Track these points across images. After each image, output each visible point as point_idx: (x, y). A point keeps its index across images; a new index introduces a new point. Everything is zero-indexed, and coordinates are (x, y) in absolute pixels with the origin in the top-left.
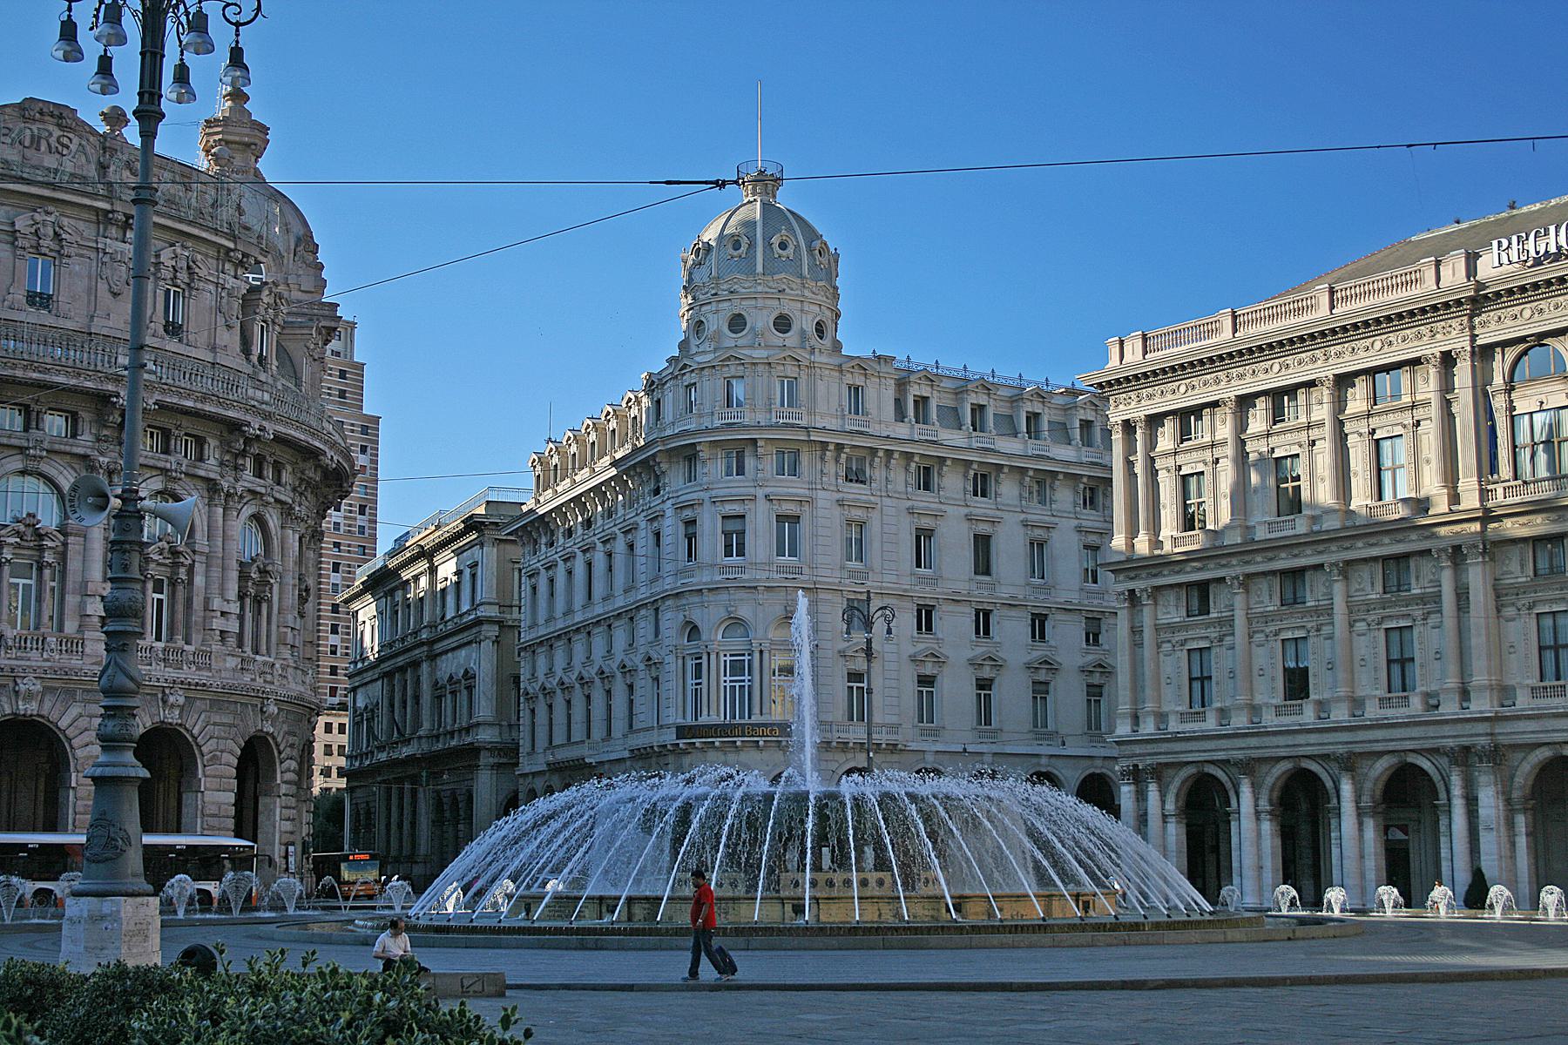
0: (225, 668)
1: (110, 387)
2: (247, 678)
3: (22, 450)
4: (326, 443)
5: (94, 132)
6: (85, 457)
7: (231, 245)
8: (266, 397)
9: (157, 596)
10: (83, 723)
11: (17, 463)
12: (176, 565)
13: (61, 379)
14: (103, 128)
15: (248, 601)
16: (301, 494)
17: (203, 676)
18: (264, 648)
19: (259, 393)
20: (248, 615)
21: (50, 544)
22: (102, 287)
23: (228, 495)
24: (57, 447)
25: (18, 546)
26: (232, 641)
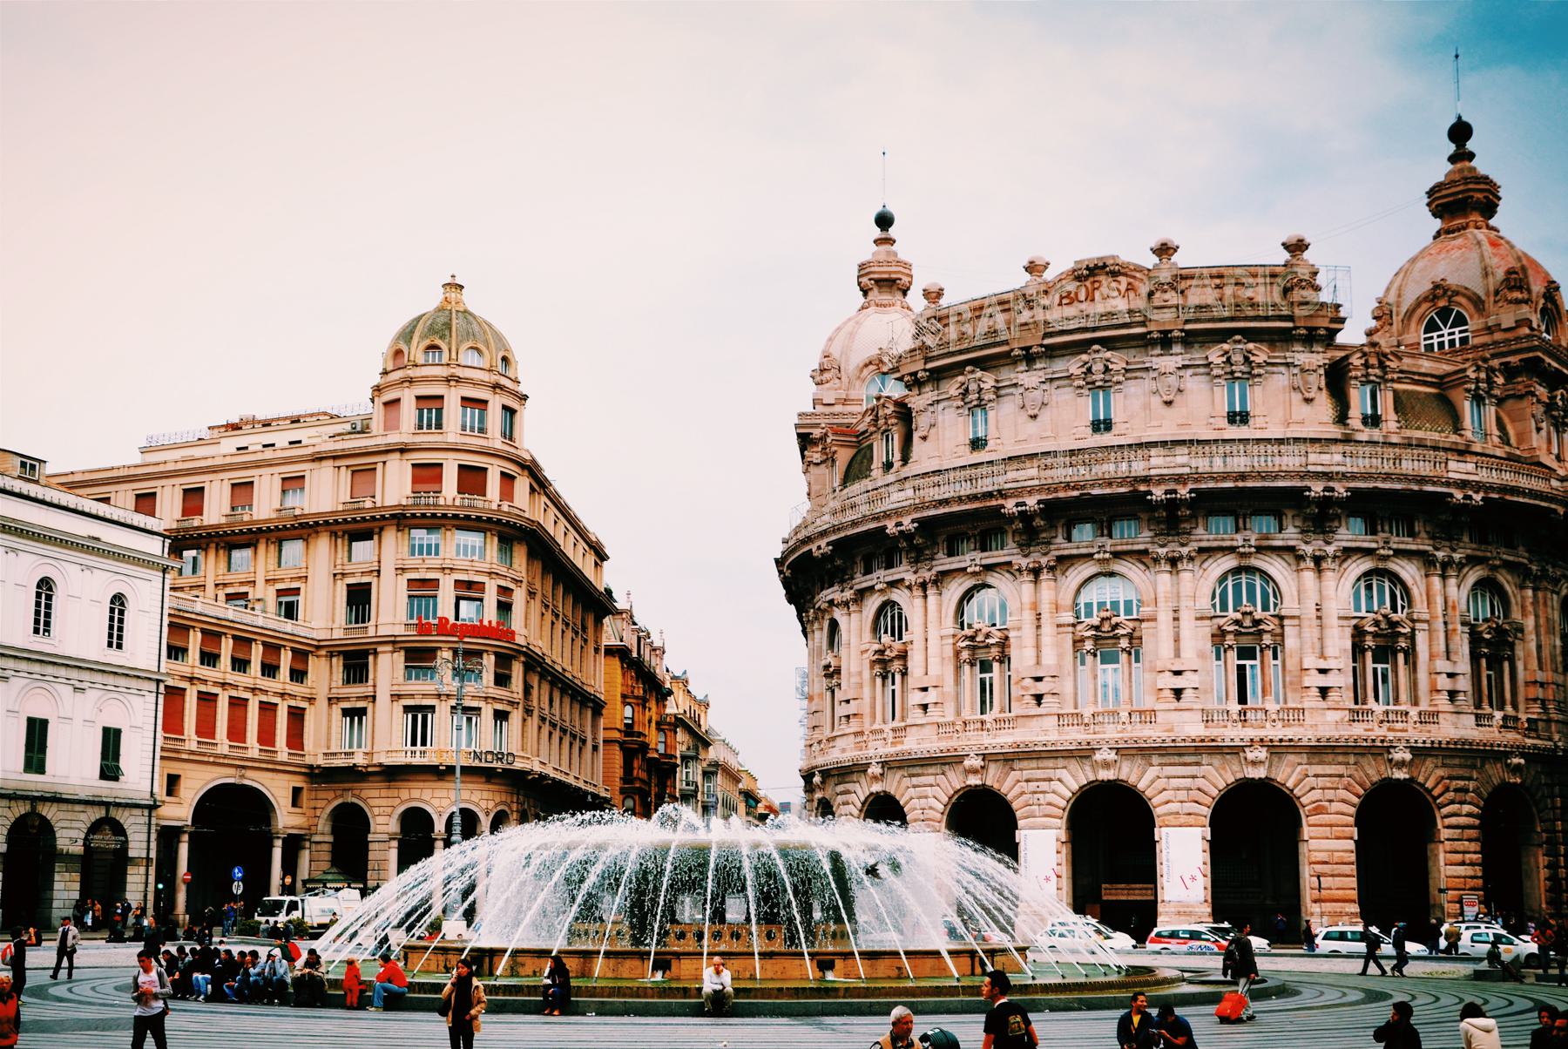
0: (1328, 723)
1: (1142, 488)
3: (1090, 556)
4: (1448, 484)
5: (1139, 269)
6: (1146, 552)
7: (1290, 325)
8: (1338, 458)
9: (1248, 663)
10: (1161, 783)
11: (1089, 569)
12: (1260, 633)
13: (1096, 491)
14: (1150, 261)
15: (1369, 655)
16: (1450, 540)
18: (1403, 696)
19: (1325, 458)
20: (1370, 665)
21: (1120, 631)
22: (1156, 401)
24: (1119, 548)
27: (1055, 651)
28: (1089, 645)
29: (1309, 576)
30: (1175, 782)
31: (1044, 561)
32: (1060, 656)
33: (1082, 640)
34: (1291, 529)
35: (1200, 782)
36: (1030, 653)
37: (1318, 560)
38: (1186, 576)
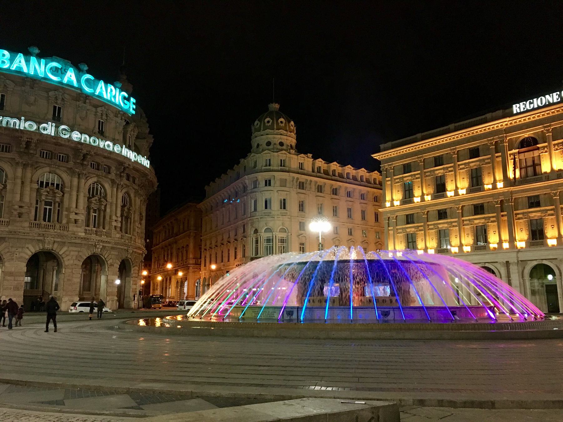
2: (123, 240)
9: (94, 214)
10: (67, 253)
11: (47, 169)
15: (124, 218)
17: (108, 239)
20: (124, 222)
23: (118, 185)
25: (47, 195)
26: (118, 229)
27: (29, 196)
28: (43, 198)
29: (115, 189)
30: (72, 253)
31: (30, 162)
32: (30, 199)
33: (41, 195)
34: (113, 174)
35: (81, 254)
36: (18, 197)
37: (118, 185)
38: (83, 181)
